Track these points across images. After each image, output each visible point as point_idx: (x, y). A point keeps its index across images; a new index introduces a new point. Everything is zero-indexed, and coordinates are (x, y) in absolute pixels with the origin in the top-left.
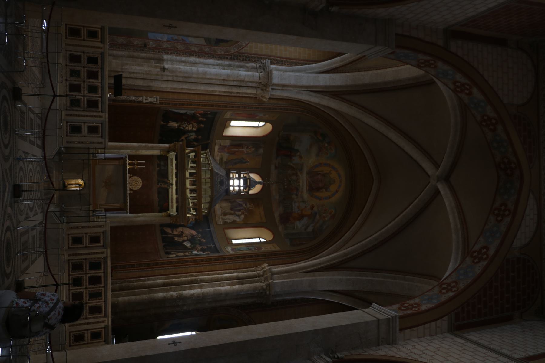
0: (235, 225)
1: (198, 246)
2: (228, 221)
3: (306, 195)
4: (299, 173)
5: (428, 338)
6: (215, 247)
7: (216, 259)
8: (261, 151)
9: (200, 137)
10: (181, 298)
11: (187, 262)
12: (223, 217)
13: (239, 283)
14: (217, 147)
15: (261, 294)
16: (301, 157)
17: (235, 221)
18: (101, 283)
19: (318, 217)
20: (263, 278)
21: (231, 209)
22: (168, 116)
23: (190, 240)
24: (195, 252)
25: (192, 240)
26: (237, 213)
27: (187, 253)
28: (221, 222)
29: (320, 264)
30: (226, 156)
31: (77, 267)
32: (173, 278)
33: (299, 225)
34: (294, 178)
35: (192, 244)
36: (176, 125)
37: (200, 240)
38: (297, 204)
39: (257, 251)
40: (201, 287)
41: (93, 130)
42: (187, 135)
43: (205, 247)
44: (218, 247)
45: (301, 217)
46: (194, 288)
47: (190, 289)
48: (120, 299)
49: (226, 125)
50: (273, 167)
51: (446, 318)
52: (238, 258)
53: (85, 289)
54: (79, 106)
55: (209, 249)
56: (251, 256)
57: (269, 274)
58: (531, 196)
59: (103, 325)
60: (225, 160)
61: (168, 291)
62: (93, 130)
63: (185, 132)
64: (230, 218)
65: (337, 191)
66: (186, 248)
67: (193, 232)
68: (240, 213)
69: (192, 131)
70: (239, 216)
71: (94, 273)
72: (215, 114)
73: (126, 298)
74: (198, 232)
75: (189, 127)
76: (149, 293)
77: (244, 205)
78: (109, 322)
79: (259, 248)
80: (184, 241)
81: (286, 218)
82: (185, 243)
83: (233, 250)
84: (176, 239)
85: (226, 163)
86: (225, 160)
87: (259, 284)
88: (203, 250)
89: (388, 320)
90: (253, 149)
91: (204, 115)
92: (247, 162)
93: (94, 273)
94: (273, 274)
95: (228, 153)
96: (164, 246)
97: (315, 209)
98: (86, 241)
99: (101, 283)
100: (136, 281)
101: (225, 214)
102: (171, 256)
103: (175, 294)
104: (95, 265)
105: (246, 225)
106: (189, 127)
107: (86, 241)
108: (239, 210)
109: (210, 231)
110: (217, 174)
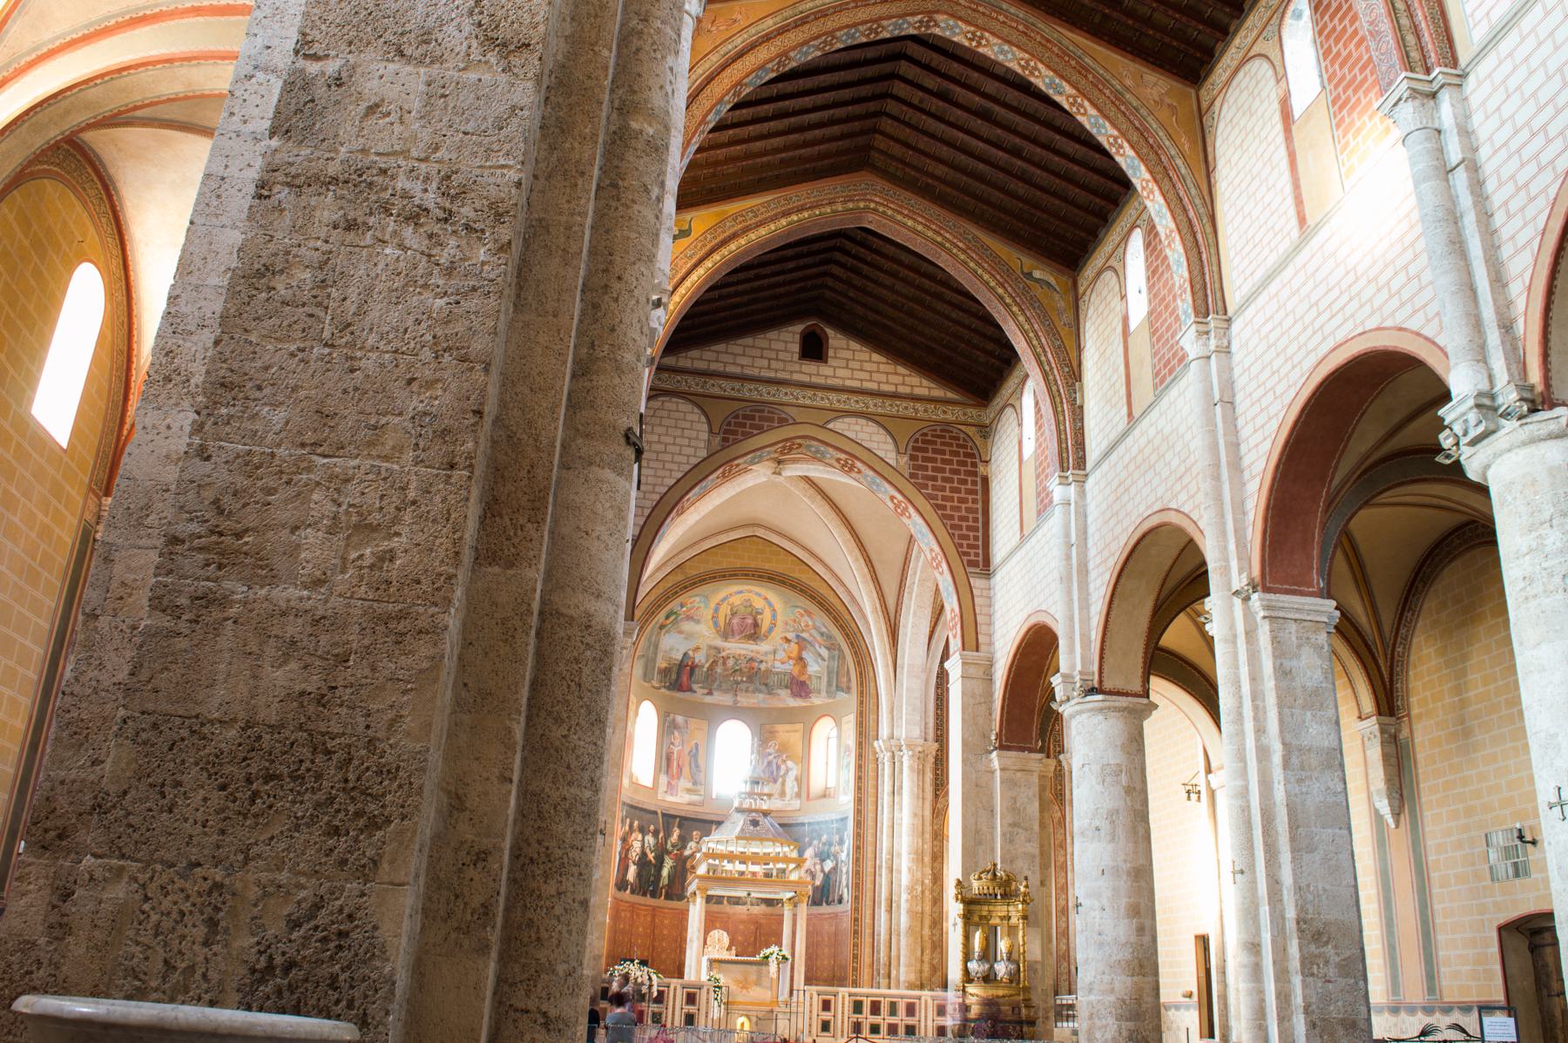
0: (803, 780)
1: (833, 849)
2: (796, 790)
3: (764, 647)
4: (724, 654)
5: (992, 592)
6: (837, 821)
7: (859, 824)
8: (680, 719)
9: (652, 827)
10: (911, 890)
11: (857, 873)
12: (788, 797)
13: (900, 794)
14: (670, 798)
15: (921, 757)
16: (697, 649)
17: (796, 779)
18: (879, 1002)
19: (804, 635)
20: (897, 753)
21: (775, 781)
22: (622, 885)
23: (823, 861)
24: (843, 856)
25: (822, 857)
26: (782, 773)
27: (844, 870)
28: (796, 804)
29: (884, 655)
30: (684, 783)
31: (857, 1028)
32: (880, 896)
33: (814, 668)
34: (730, 662)
35: (828, 857)
36: (632, 870)
37: (824, 844)
38: (778, 664)
39: (853, 755)
40: (899, 855)
41: (691, 999)
42: (648, 851)
43: (836, 838)
44: (839, 817)
45: (800, 659)
46: (900, 865)
47: (900, 872)
48: (902, 978)
49: (636, 786)
50: (708, 699)
51: (973, 581)
52: (859, 788)
53: (884, 1019)
54: (660, 1014)
55: (840, 831)
56: (859, 767)
57: (893, 742)
58: (831, 426)
59: (930, 1002)
60: (689, 785)
61: (899, 907)
62: (691, 999)
63: (644, 854)
64: (791, 786)
65: (766, 599)
66: (835, 869)
67: (809, 853)
68: (783, 767)
69: (643, 840)
70: (788, 770)
71: (866, 1008)
72: (624, 803)
73: (902, 969)
74: (810, 845)
75: (637, 846)
76: (899, 935)
77: (771, 758)
78: (926, 994)
79: (848, 748)
80: (822, 870)
81: (800, 687)
82: (827, 869)
83: (845, 793)
84: (818, 883)
85: (695, 783)
86: (689, 785)
87: (906, 760)
88: (841, 842)
89: (963, 663)
90: (676, 733)
91: (623, 822)
92: (697, 745)
93: (866, 1008)
94: (892, 737)
95: (678, 778)
96: (828, 903)
97: (791, 636)
98: (827, 1016)
99: (879, 1002)
100: (879, 953)
101: (783, 794)
102: (845, 896)
103: (904, 897)
104: (858, 1007)
105: (805, 759)
106: (637, 846)
107: (827, 1016)
108: (778, 768)
109: (809, 823)
110: (742, 830)
